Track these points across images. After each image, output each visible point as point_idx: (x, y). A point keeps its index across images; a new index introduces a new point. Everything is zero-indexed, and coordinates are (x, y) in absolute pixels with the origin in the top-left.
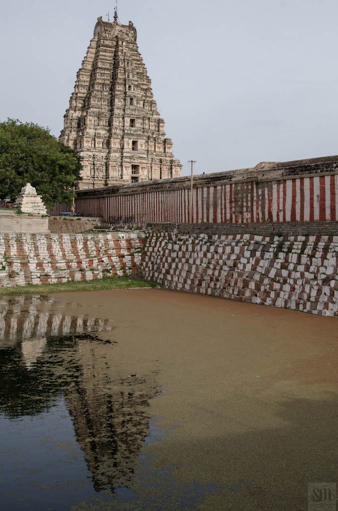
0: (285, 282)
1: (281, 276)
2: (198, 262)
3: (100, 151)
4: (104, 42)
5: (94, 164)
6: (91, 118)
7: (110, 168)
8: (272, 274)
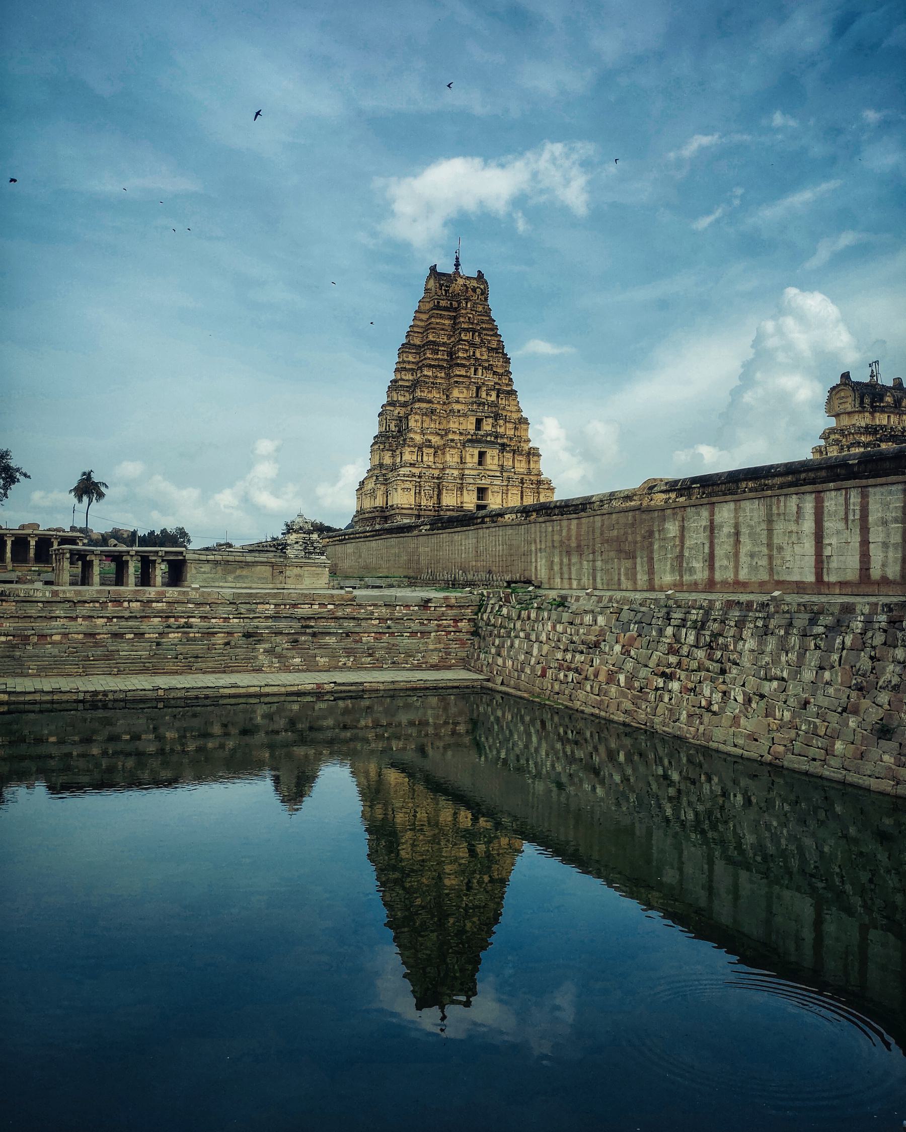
0: (668, 677)
1: (669, 665)
2: (543, 638)
4: (438, 303)
5: (420, 486)
7: (444, 491)
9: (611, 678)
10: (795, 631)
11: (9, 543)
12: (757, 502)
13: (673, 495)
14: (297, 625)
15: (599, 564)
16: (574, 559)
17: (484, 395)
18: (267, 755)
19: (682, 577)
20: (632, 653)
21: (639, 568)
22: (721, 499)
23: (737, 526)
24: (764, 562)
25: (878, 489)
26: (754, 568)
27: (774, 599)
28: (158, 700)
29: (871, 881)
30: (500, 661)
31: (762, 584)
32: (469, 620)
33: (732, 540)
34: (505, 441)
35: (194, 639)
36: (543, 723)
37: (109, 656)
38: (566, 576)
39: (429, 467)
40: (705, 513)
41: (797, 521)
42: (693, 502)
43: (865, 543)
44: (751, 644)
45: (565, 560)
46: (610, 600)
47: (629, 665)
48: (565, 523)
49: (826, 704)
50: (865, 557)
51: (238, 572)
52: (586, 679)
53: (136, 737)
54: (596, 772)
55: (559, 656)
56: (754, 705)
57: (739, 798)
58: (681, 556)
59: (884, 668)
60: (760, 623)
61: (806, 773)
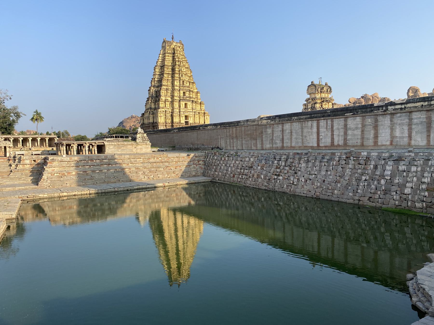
0: (279, 175)
2: (232, 165)
8: (272, 171)
9: (259, 176)
10: (318, 161)
11: (47, 141)
12: (298, 123)
13: (269, 121)
15: (244, 142)
16: (235, 140)
17: (185, 84)
18: (143, 208)
19: (273, 145)
20: (264, 169)
21: (258, 143)
22: (286, 122)
23: (291, 130)
24: (300, 141)
25: (337, 119)
26: (297, 143)
27: (309, 152)
28: (115, 192)
29: (342, 227)
30: (217, 173)
31: (300, 147)
33: (289, 134)
34: (193, 99)
35: (118, 172)
36: (234, 191)
37: (92, 178)
38: (232, 146)
39: (168, 109)
40: (280, 126)
41: (311, 129)
42: (276, 123)
43: (332, 135)
44: (304, 165)
45: (232, 141)
46: (254, 153)
47: (264, 172)
48: (231, 129)
49: (330, 181)
50: (333, 139)
51: (122, 148)
52: (249, 177)
53: (102, 205)
54: (252, 204)
55: (239, 171)
56: (308, 182)
57: (303, 208)
58: (272, 139)
59: (346, 170)
60: (306, 159)
61: (327, 200)
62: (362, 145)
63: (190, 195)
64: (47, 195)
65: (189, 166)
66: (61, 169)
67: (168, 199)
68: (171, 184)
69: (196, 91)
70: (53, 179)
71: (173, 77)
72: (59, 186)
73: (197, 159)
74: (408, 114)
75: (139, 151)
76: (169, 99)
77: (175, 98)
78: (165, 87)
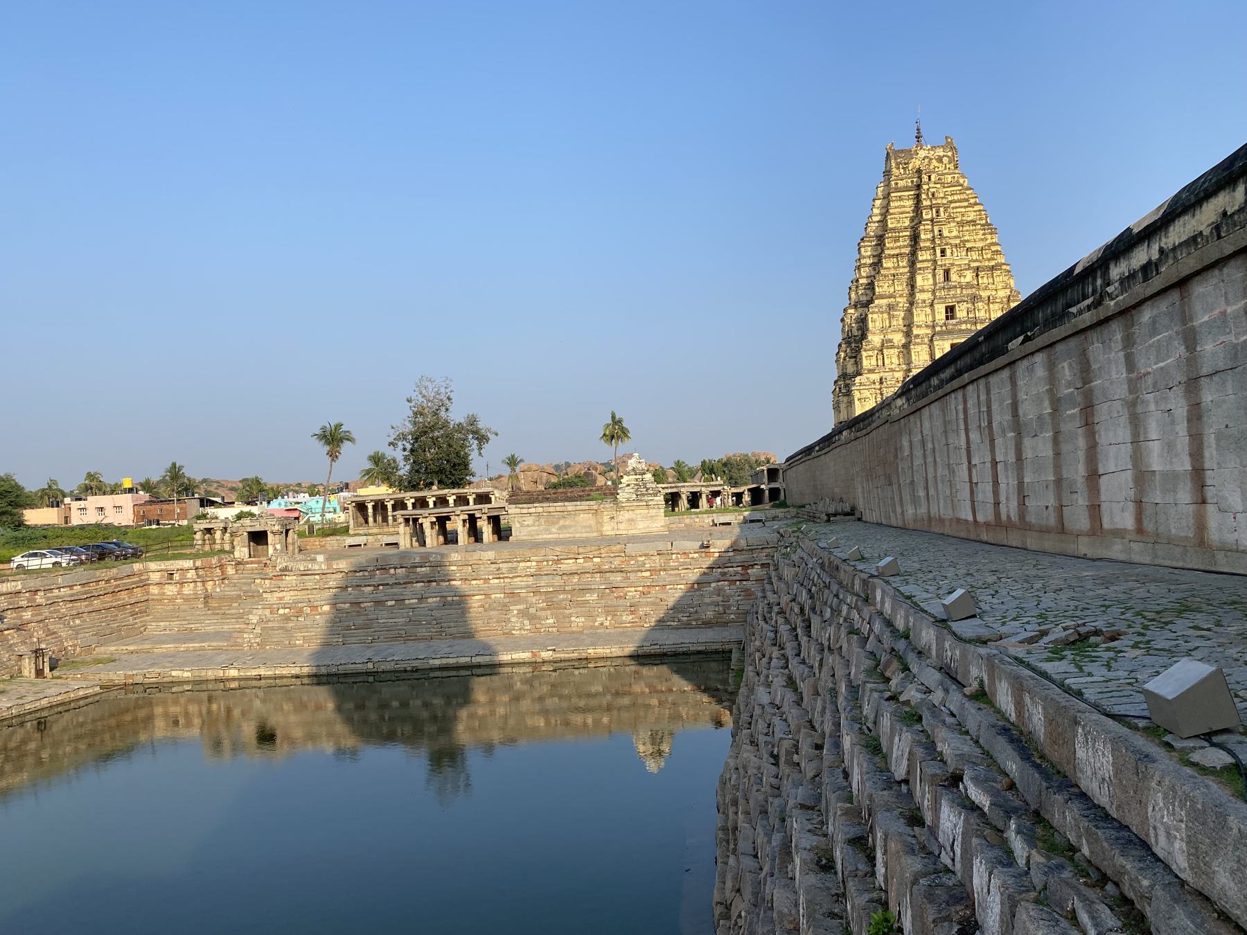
3: (892, 370)
6: (875, 316)
14: (558, 581)
17: (954, 277)
18: (542, 724)
28: (368, 673)
32: (762, 565)
35: (452, 604)
39: (892, 370)
43: (995, 463)
51: (562, 522)
53: (404, 705)
62: (1062, 529)
63: (704, 691)
64: (189, 674)
65: (700, 584)
66: (301, 595)
67: (626, 701)
68: (562, 656)
69: (1002, 294)
70: (270, 625)
71: (912, 264)
72: (278, 643)
73: (739, 558)
74: (1175, 296)
75: (624, 530)
76: (899, 339)
77: (915, 331)
78: (884, 302)
